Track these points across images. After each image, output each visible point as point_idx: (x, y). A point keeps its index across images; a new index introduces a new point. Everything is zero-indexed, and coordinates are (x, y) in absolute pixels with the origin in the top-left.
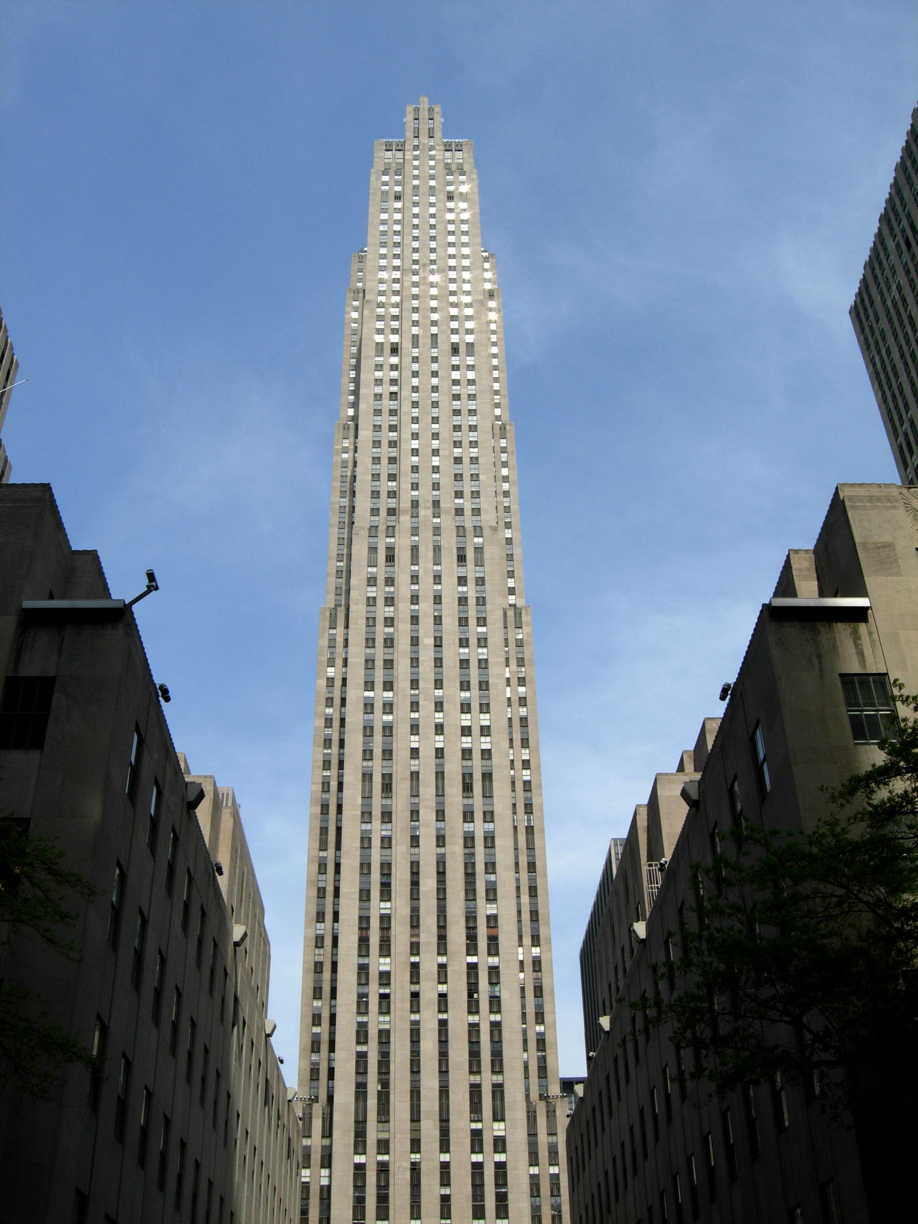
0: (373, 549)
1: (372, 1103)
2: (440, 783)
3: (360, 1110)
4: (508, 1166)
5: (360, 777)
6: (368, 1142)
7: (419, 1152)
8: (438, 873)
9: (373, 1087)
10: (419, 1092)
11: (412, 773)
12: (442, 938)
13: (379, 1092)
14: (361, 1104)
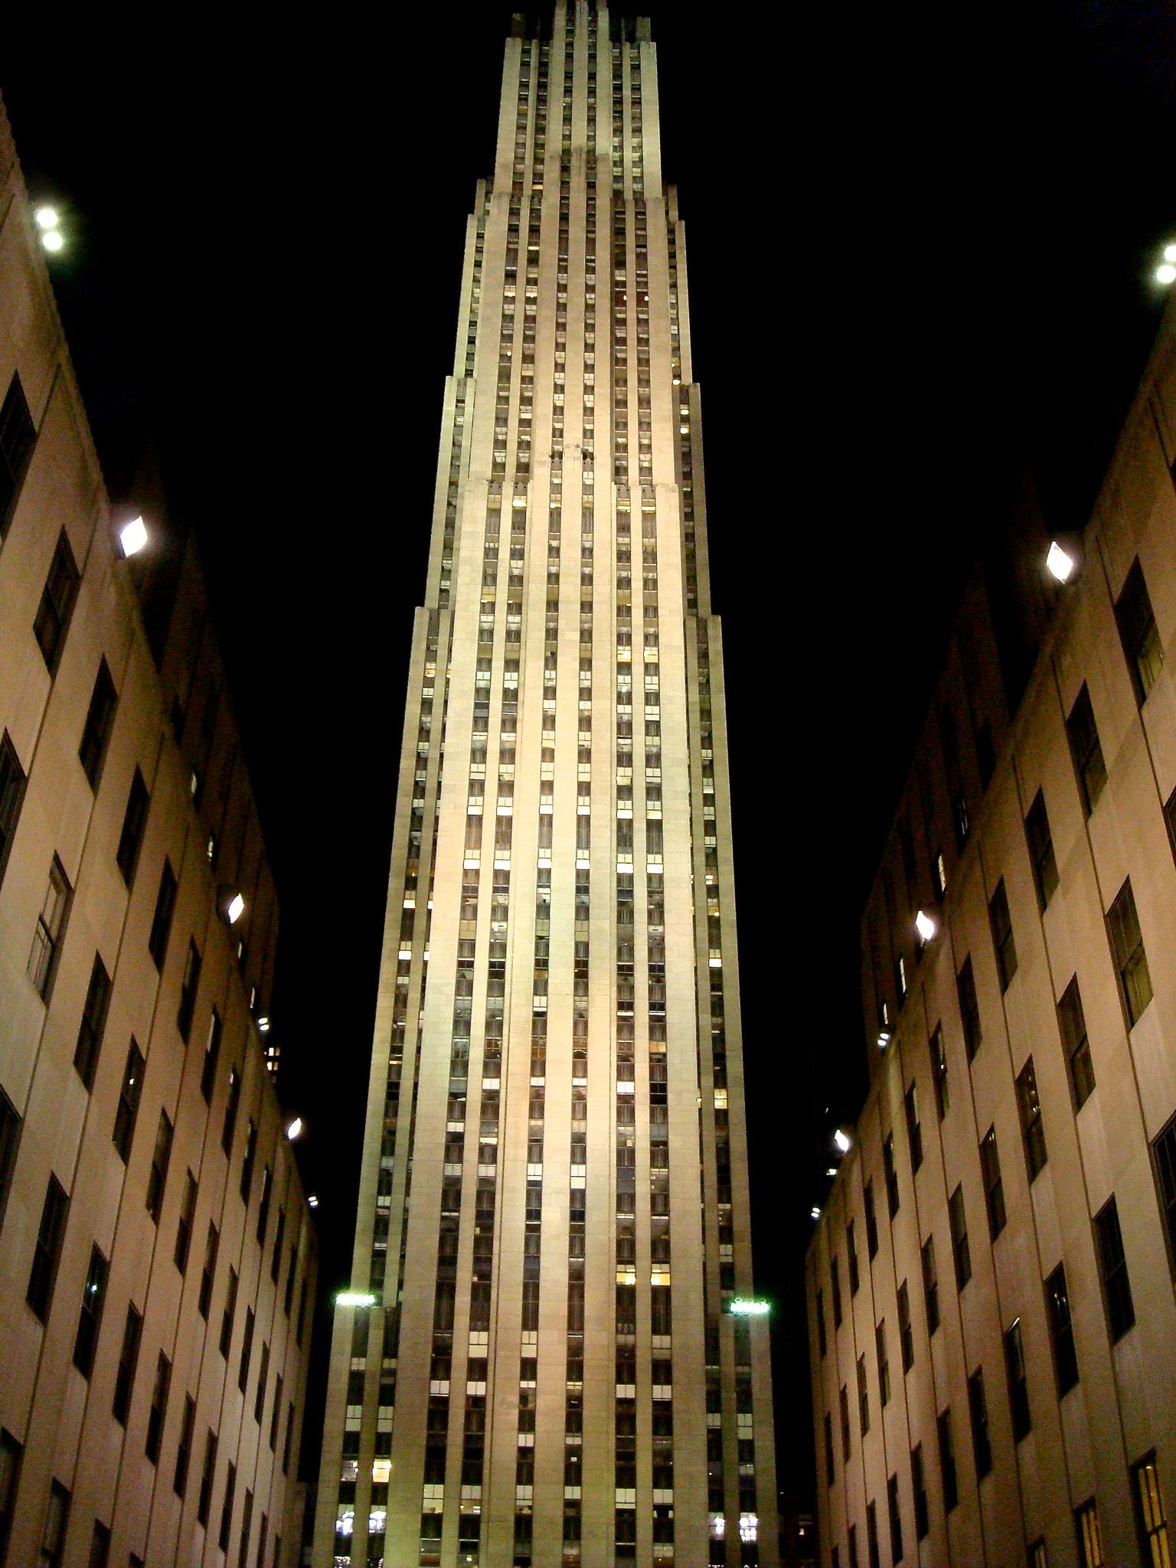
0: (494, 513)
1: (463, 1300)
2: (584, 832)
3: (444, 1311)
4: (675, 1407)
5: (465, 820)
6: (454, 1361)
7: (534, 1377)
8: (578, 964)
9: (468, 1231)
10: (537, 1287)
11: (542, 817)
12: (580, 1056)
13: (474, 1284)
14: (445, 1302)
